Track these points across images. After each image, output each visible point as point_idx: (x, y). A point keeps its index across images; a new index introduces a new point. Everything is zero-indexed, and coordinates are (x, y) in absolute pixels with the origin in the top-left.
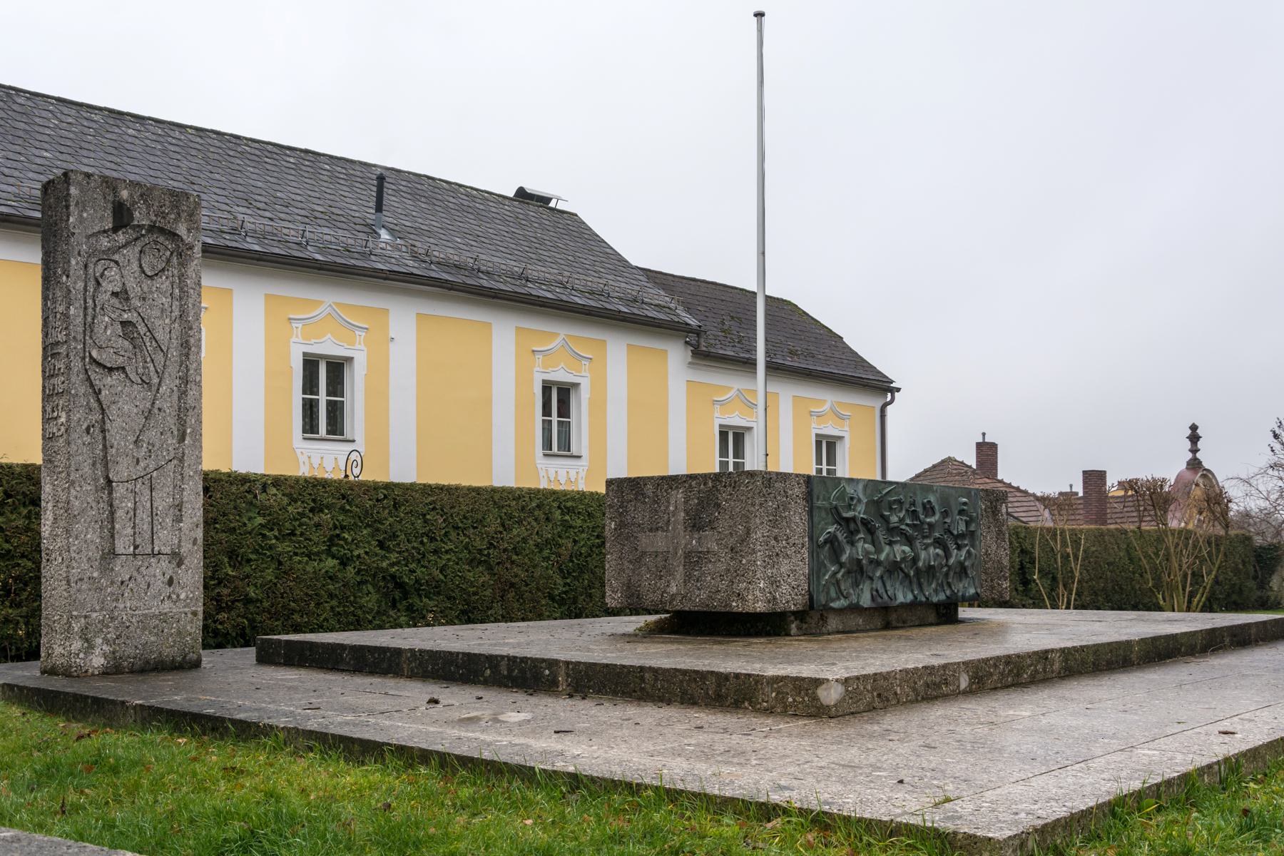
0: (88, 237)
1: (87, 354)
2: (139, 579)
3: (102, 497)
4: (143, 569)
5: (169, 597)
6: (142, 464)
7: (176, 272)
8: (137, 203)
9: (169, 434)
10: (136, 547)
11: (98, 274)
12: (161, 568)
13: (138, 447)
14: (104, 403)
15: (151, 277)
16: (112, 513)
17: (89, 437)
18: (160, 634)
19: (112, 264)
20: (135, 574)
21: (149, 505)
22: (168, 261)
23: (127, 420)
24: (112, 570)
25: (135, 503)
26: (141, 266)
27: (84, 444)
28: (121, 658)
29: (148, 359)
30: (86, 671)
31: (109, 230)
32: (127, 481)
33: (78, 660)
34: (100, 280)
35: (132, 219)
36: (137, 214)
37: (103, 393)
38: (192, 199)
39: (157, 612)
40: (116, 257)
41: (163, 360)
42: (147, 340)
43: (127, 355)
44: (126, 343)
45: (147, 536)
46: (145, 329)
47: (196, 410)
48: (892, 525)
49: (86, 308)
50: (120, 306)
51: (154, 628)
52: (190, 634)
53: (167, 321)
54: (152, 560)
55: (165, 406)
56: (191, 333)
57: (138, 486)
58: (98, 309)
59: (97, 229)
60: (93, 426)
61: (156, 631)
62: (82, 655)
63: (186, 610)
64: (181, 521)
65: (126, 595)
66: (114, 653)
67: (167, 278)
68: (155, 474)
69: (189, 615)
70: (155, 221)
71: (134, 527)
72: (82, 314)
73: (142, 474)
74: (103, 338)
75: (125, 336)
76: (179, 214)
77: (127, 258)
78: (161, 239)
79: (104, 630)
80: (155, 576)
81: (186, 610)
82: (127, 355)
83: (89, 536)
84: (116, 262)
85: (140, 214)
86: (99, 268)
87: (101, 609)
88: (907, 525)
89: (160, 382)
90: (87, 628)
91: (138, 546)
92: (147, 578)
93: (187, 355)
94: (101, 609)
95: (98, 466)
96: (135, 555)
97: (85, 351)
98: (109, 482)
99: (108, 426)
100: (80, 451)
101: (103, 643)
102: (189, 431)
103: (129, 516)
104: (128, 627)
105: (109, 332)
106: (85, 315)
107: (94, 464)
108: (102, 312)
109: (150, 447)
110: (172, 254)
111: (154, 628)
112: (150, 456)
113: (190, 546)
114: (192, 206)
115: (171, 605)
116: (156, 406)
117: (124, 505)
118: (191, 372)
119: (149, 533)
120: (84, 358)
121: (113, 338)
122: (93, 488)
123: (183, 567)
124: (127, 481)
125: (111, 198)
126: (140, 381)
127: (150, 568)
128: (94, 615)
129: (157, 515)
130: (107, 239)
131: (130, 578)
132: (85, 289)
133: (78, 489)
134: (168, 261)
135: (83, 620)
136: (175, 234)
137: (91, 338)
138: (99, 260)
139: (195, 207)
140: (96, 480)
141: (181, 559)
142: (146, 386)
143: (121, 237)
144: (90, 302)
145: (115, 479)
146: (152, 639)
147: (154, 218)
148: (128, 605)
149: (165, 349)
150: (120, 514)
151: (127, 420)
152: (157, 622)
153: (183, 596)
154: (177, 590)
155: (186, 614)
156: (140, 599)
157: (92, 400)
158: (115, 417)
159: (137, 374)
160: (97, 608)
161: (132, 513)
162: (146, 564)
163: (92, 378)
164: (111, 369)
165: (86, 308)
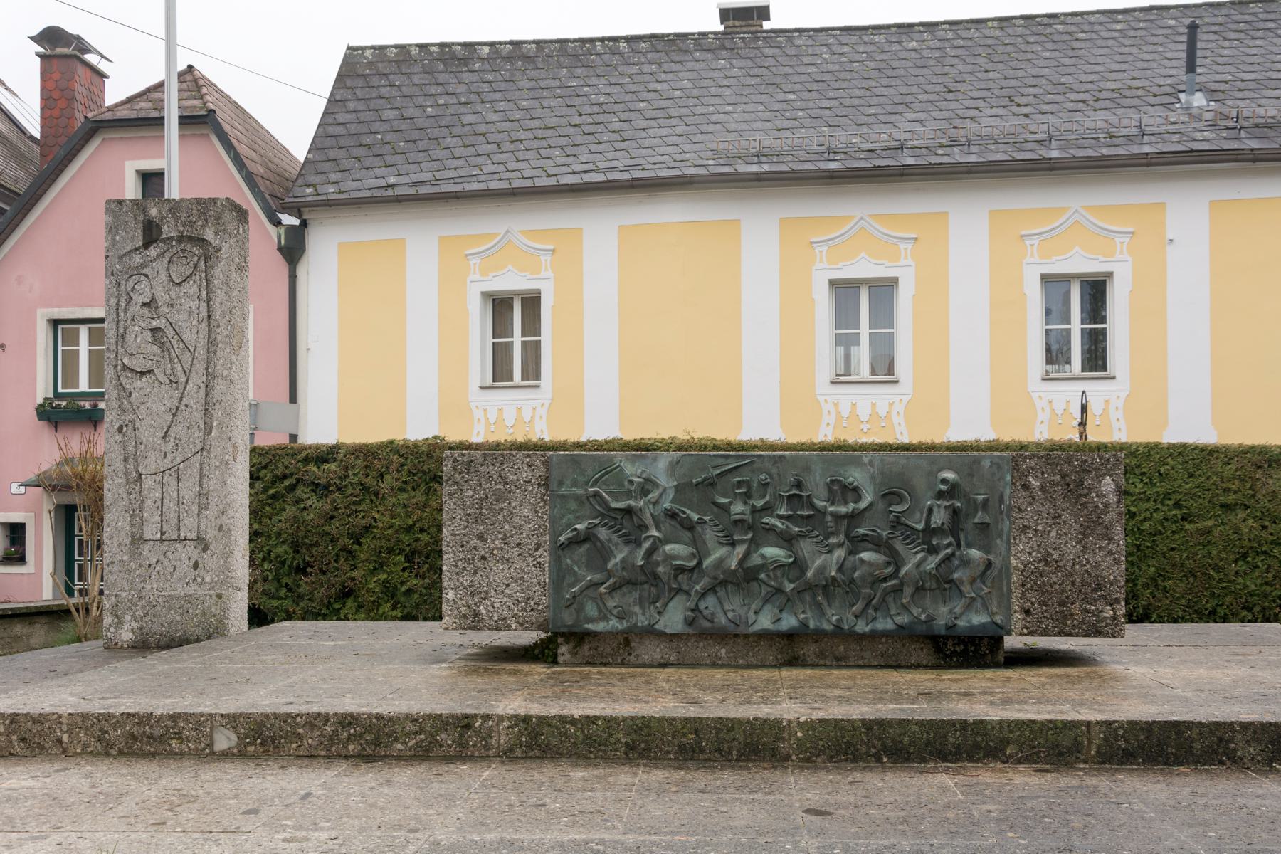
0: (121, 257)
1: (119, 362)
2: (166, 562)
3: (134, 489)
4: (169, 554)
5: (194, 580)
6: (169, 457)
7: (203, 275)
8: (165, 218)
9: (196, 427)
10: (163, 534)
11: (129, 289)
12: (187, 553)
13: (165, 442)
14: (135, 404)
15: (179, 284)
17: (121, 435)
18: (185, 614)
19: (142, 278)
20: (162, 558)
21: (175, 494)
22: (196, 266)
23: (156, 418)
24: (141, 554)
25: (163, 493)
26: (170, 276)
27: (116, 442)
28: (147, 634)
29: (176, 360)
30: (116, 644)
31: (140, 247)
32: (155, 474)
33: (109, 634)
34: (131, 294)
35: (161, 233)
36: (165, 228)
37: (133, 395)
38: (219, 203)
39: (182, 594)
40: (146, 271)
41: (190, 359)
42: (174, 342)
43: (155, 358)
44: (155, 348)
45: (174, 523)
46: (173, 333)
47: (222, 403)
48: (733, 518)
49: (118, 322)
50: (150, 315)
51: (180, 608)
52: (215, 616)
53: (195, 322)
54: (178, 545)
55: (192, 402)
56: (218, 331)
57: (165, 478)
58: (129, 321)
59: (128, 248)
60: (127, 426)
61: (181, 611)
62: (112, 630)
63: (211, 592)
64: (207, 509)
65: (153, 577)
66: (141, 629)
67: (194, 282)
68: (181, 466)
69: (214, 598)
70: (183, 231)
71: (161, 515)
72: (114, 327)
73: (169, 467)
74: (134, 346)
75: (155, 341)
76: (206, 220)
77: (156, 270)
78: (189, 247)
79: (133, 608)
80: (180, 560)
81: (211, 592)
82: (155, 358)
83: (120, 524)
84: (146, 276)
85: (168, 227)
86: (131, 283)
87: (130, 589)
88: (780, 517)
89: (187, 380)
90: (117, 606)
91: (165, 532)
92: (173, 562)
93: (215, 352)
94: (130, 589)
95: (131, 460)
96: (161, 541)
97: (117, 359)
99: (138, 425)
100: (112, 449)
101: (131, 620)
102: (215, 424)
103: (156, 505)
104: (154, 606)
105: (139, 340)
106: (118, 327)
107: (125, 460)
108: (133, 323)
109: (177, 441)
110: (199, 259)
111: (180, 608)
112: (177, 450)
113: (216, 532)
114: (219, 210)
115: (196, 587)
116: (183, 403)
117: (152, 495)
118: (218, 367)
120: (116, 366)
121: (143, 345)
122: (124, 481)
123: (208, 552)
124: (155, 474)
125: (140, 218)
126: (168, 381)
127: (176, 553)
128: (124, 594)
129: (183, 503)
130: (139, 256)
131: (157, 562)
132: (118, 304)
133: (111, 482)
134: (196, 266)
135: (113, 598)
136: (204, 240)
137: (122, 347)
138: (131, 276)
139: (223, 210)
140: (127, 473)
141: (206, 544)
142: (174, 385)
143: (153, 251)
144: (122, 314)
145: (144, 472)
146: (178, 618)
147: (182, 229)
148: (155, 586)
149: (192, 349)
150: (148, 503)
151: (156, 418)
152: (183, 602)
153: (208, 579)
154: (203, 573)
155: (211, 596)
156: (166, 581)
157: (125, 403)
158: (144, 416)
159: (165, 375)
160: (127, 588)
161: (160, 502)
162: (172, 549)
163: (124, 383)
164: (142, 373)
165: (118, 322)
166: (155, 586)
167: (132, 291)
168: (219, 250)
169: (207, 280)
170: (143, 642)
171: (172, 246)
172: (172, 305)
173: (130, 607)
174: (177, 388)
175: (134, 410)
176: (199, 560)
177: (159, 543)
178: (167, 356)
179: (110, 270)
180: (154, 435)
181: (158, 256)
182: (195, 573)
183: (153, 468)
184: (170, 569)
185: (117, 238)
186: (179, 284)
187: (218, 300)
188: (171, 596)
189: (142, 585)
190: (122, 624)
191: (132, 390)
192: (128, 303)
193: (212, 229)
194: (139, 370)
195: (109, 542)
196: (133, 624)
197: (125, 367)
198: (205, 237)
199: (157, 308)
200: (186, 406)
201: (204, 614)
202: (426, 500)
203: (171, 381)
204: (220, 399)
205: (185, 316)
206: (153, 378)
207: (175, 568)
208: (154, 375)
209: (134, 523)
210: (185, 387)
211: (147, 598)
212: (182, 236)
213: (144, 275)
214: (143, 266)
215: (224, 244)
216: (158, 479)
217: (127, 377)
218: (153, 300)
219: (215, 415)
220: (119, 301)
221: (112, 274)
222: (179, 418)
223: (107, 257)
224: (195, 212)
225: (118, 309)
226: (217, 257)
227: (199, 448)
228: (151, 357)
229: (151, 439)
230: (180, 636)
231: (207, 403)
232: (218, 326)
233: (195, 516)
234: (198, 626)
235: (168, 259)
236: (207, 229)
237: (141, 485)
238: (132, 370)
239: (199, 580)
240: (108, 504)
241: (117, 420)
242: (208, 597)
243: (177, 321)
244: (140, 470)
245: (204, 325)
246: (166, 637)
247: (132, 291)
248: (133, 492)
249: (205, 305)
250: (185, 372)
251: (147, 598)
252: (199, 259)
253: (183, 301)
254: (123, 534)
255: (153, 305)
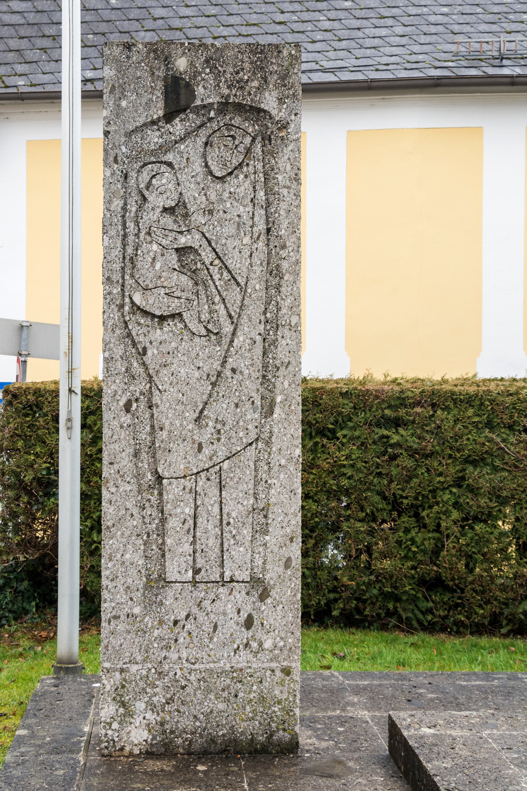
0: (129, 134)
1: (127, 300)
2: (201, 617)
3: (149, 500)
4: (206, 603)
5: (247, 645)
6: (206, 451)
7: (260, 166)
8: (200, 73)
9: (248, 405)
10: (197, 571)
11: (142, 186)
13: (200, 427)
14: (151, 367)
15: (221, 179)
16: (163, 521)
17: (129, 416)
18: (232, 699)
19: (164, 168)
20: (195, 610)
21: (216, 510)
22: (248, 151)
23: (185, 389)
24: (161, 604)
25: (196, 507)
26: (207, 166)
27: (122, 427)
28: (172, 732)
29: (217, 299)
30: (122, 749)
31: (159, 119)
32: (185, 477)
33: (110, 732)
34: (146, 193)
35: (193, 97)
36: (200, 90)
37: (149, 353)
38: (285, 53)
39: (228, 667)
40: (169, 157)
41: (239, 297)
42: (214, 271)
43: (184, 295)
44: (184, 279)
45: (214, 554)
46: (212, 255)
47: (290, 368)
49: (125, 236)
50: (175, 227)
51: (223, 690)
52: (279, 703)
53: (247, 240)
54: (221, 590)
55: (242, 364)
56: (283, 253)
57: (200, 483)
58: (142, 235)
59: (141, 120)
60: (137, 400)
61: (225, 694)
62: (115, 726)
63: (274, 665)
64: (266, 532)
65: (181, 640)
66: (162, 724)
67: (246, 176)
68: (226, 465)
69: (278, 673)
70: (229, 96)
71: (194, 543)
72: (119, 244)
73: (207, 466)
74: (151, 275)
75: (183, 269)
76: (265, 79)
77: (185, 156)
78: (237, 121)
79: (148, 690)
80: (225, 614)
81: (274, 665)
82: (184, 295)
83: (128, 556)
84: (170, 165)
85: (205, 88)
86: (145, 176)
87: (144, 661)
89: (235, 330)
90: (123, 687)
91: (200, 570)
92: (212, 616)
93: (278, 287)
94: (144, 661)
95: (144, 455)
96: (194, 583)
97: (123, 296)
98: (159, 478)
99: (156, 399)
100: (115, 437)
101: (146, 709)
102: (279, 399)
103: (186, 526)
104: (183, 688)
105: (158, 266)
106: (124, 246)
107: (136, 454)
108: (149, 239)
109: (219, 426)
110: (254, 140)
111: (223, 690)
112: (219, 440)
113: (281, 569)
114: (286, 64)
115: (250, 657)
116: (228, 366)
117: (179, 510)
118: (284, 311)
119: (217, 550)
120: (121, 307)
121: (164, 274)
122: (135, 487)
123: (269, 601)
124: (185, 477)
125: (161, 74)
126: (204, 332)
127: (218, 603)
128: (134, 668)
129: (228, 524)
130: (158, 133)
131: (188, 616)
132: (124, 209)
133: (113, 490)
134: (248, 151)
135: (117, 674)
136: (260, 110)
137: (132, 276)
138: (145, 165)
139: (291, 64)
140: (138, 476)
141: (265, 589)
142: (213, 337)
143: (179, 127)
144: (131, 225)
145: (166, 474)
146: (221, 706)
147: (226, 92)
148: (184, 655)
149: (242, 282)
150: (172, 523)
151: (185, 389)
152: (228, 681)
153: (268, 644)
154: (259, 635)
155: (273, 671)
156: (202, 647)
157: (135, 364)
158: (165, 387)
159: (200, 321)
160: (139, 658)
161: (191, 522)
162: (212, 596)
163: (134, 333)
164: (162, 318)
165: (125, 236)
166: (184, 655)
167: (147, 188)
168: (285, 126)
169: (265, 174)
170: (165, 744)
171: (210, 120)
172: (211, 212)
173: (144, 689)
174: (219, 343)
175: (151, 377)
176: (254, 613)
177: (189, 587)
178: (202, 293)
179: (112, 153)
180: (181, 415)
181: (188, 135)
182: (247, 634)
183: (181, 468)
184: (208, 628)
185: (124, 104)
186: (221, 179)
187: (283, 206)
188: (211, 671)
189: (164, 653)
190: (132, 716)
191: (148, 344)
192: (140, 208)
193: (275, 94)
194: (158, 313)
195: (111, 585)
196: (149, 715)
197: (136, 309)
198: (262, 106)
199: (186, 216)
200: (234, 370)
201: (262, 699)
202: (313, 459)
203: (208, 330)
204: (286, 361)
205: (231, 230)
206: (180, 325)
207: (215, 627)
208: (182, 320)
209: (149, 553)
210: (232, 341)
211: (171, 674)
212: (227, 103)
213: (165, 163)
214: (164, 148)
215: (293, 117)
216: (188, 485)
217: (139, 324)
218: (181, 203)
219: (278, 385)
220: (125, 204)
221: (116, 161)
222: (222, 389)
223: (106, 133)
224: (247, 65)
225: (123, 216)
226: (282, 139)
227: (253, 436)
228: (178, 294)
229: (178, 423)
230: (223, 735)
231: (265, 367)
232: (283, 247)
233: (248, 544)
234: (253, 718)
235: (204, 140)
236: (267, 94)
237: (161, 494)
238: (146, 313)
239: (254, 645)
240: (110, 524)
241: (124, 391)
242: (268, 673)
243: (219, 238)
244: (160, 470)
245: (261, 244)
246: (201, 736)
247: (147, 188)
248: (147, 505)
249: (263, 212)
250: (230, 316)
251: (171, 674)
252: (254, 140)
253: (228, 205)
254: (133, 572)
255: (180, 211)
